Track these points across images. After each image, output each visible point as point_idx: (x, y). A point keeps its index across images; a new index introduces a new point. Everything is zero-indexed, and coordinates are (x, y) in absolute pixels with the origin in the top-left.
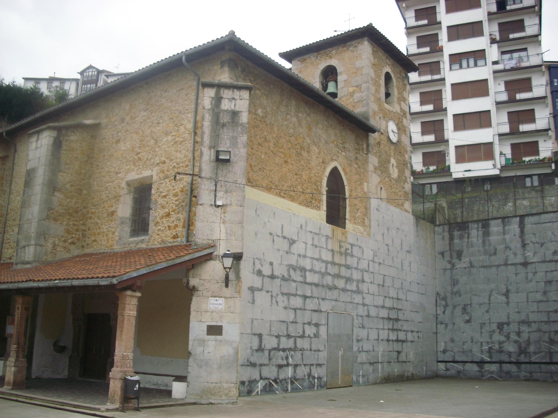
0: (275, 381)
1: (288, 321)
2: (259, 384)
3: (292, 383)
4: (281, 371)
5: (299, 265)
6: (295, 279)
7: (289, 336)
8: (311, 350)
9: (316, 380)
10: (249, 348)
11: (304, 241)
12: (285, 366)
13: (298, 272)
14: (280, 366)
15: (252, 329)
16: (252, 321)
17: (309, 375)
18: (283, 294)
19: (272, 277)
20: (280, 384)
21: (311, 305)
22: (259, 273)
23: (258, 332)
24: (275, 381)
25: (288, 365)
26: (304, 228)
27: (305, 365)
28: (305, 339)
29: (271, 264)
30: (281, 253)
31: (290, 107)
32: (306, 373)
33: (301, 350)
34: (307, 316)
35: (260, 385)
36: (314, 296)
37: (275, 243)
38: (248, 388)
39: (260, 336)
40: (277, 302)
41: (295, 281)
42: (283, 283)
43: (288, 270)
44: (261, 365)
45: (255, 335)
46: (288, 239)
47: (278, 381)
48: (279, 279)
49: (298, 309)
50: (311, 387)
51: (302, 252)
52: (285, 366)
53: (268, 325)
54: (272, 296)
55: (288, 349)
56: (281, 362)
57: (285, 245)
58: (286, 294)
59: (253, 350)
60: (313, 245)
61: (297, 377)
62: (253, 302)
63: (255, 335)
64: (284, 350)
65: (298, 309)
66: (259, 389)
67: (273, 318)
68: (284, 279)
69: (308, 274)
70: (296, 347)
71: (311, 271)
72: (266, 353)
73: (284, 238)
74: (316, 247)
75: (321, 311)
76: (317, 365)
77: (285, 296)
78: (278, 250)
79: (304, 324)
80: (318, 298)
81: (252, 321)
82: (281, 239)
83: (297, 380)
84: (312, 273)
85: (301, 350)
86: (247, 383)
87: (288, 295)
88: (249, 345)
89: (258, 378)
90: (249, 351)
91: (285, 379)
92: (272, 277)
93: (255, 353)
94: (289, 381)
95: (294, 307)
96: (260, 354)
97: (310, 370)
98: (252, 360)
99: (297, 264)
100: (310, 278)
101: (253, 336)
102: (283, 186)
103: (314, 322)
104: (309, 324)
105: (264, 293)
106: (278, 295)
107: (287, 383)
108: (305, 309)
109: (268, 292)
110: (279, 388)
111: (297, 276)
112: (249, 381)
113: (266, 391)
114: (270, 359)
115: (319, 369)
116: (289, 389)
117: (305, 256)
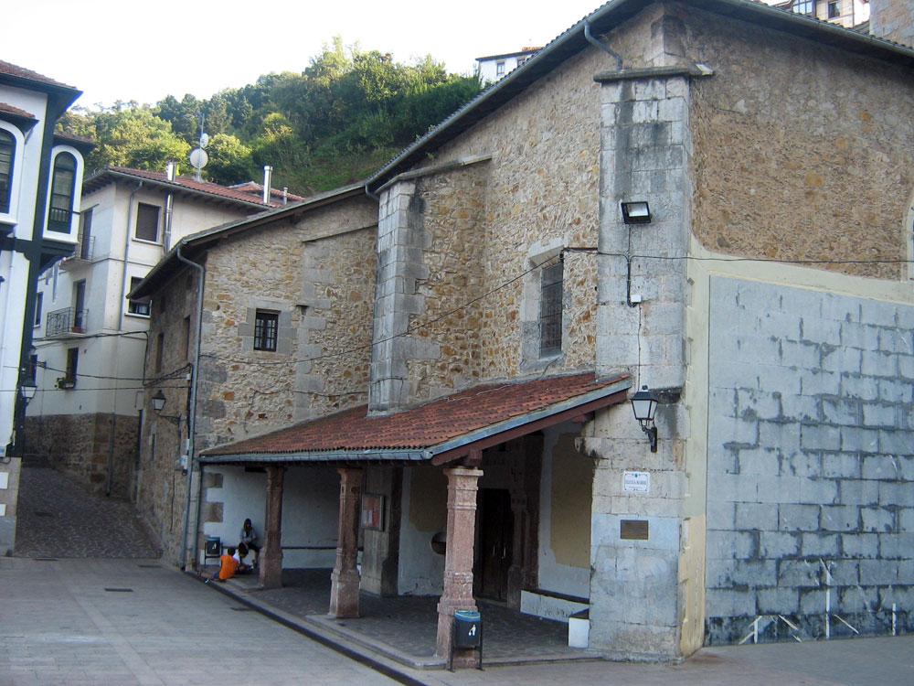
0: (793, 617)
1: (821, 502)
2: (756, 623)
3: (833, 621)
4: (804, 598)
5: (844, 394)
6: (836, 421)
7: (823, 532)
8: (879, 557)
9: (894, 616)
10: (731, 556)
11: (856, 345)
12: (816, 589)
13: (844, 408)
14: (804, 590)
15: (735, 522)
16: (736, 507)
17: (876, 607)
18: (806, 452)
19: (781, 421)
20: (804, 623)
21: (874, 469)
22: (750, 415)
23: (749, 526)
24: (793, 617)
25: (823, 587)
26: (854, 319)
27: (865, 588)
28: (864, 537)
29: (777, 396)
30: (800, 373)
31: (814, 84)
32: (867, 603)
33: (854, 558)
34: (869, 492)
35: (758, 625)
36: (884, 450)
37: (784, 355)
38: (730, 630)
39: (755, 534)
40: (793, 468)
41: (836, 426)
42: (805, 430)
43: (819, 406)
44: (757, 588)
45: (742, 531)
46: (817, 345)
47: (799, 617)
48: (798, 425)
49: (845, 479)
50: (883, 629)
51: (852, 367)
52: (816, 589)
53: (773, 513)
54: (780, 458)
55: (822, 557)
56: (804, 581)
57: (810, 358)
58: (814, 452)
59: (739, 561)
60: (878, 351)
61: (846, 611)
62: (737, 470)
63: (742, 531)
64: (812, 559)
65: (845, 479)
66: (756, 633)
67: (786, 498)
68: (807, 422)
69: (867, 409)
70: (841, 552)
71: (875, 402)
72: (771, 565)
73: (807, 343)
74: (887, 354)
75: (904, 481)
76: (895, 587)
77: (812, 457)
78: (794, 368)
79: (861, 507)
80: (894, 456)
81: (736, 507)
82: (799, 347)
83: (845, 616)
84: (879, 407)
85: (854, 558)
86: (726, 622)
87: (820, 453)
88: (730, 552)
89: (752, 611)
90: (730, 562)
91: (817, 615)
92: (781, 421)
93: (743, 566)
94: (827, 618)
95: (837, 475)
96: (755, 567)
97: (879, 596)
98: (740, 578)
99: (840, 391)
100: (872, 416)
101: (738, 534)
102: (804, 242)
103: (885, 503)
104: (874, 506)
105: (761, 452)
106: (795, 454)
107: (822, 622)
108: (861, 479)
109: (770, 450)
110: (803, 632)
111: (841, 416)
112: (731, 618)
113: (772, 637)
114: (778, 578)
115: (901, 595)
116: (828, 634)
117: (858, 376)
